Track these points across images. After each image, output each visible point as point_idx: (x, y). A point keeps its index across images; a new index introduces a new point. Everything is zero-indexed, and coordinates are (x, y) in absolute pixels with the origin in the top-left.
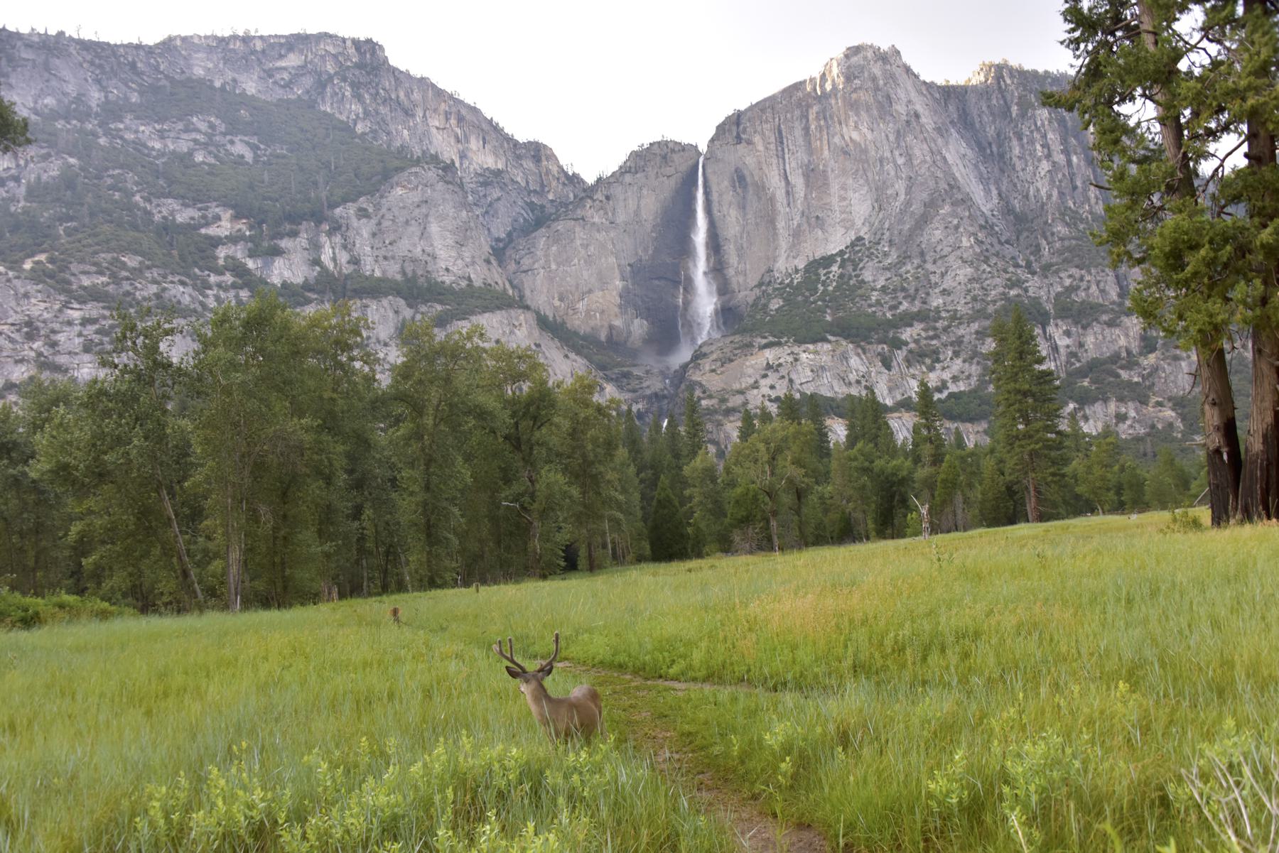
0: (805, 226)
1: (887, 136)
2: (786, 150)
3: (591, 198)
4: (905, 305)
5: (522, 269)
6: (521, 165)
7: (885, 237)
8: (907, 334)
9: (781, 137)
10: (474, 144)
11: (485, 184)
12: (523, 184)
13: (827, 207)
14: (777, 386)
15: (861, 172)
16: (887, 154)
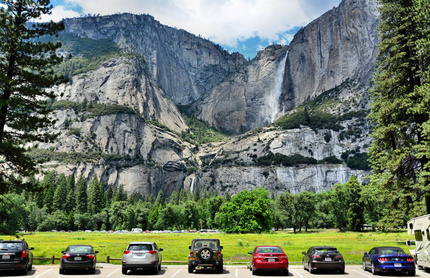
0: (326, 76)
1: (367, 28)
2: (322, 42)
3: (239, 72)
4: (353, 109)
5: (204, 103)
6: (227, 62)
7: (358, 77)
8: (344, 124)
9: (320, 36)
10: (205, 55)
11: (206, 71)
12: (227, 70)
13: (337, 66)
14: (258, 150)
15: (355, 47)
16: (367, 37)
